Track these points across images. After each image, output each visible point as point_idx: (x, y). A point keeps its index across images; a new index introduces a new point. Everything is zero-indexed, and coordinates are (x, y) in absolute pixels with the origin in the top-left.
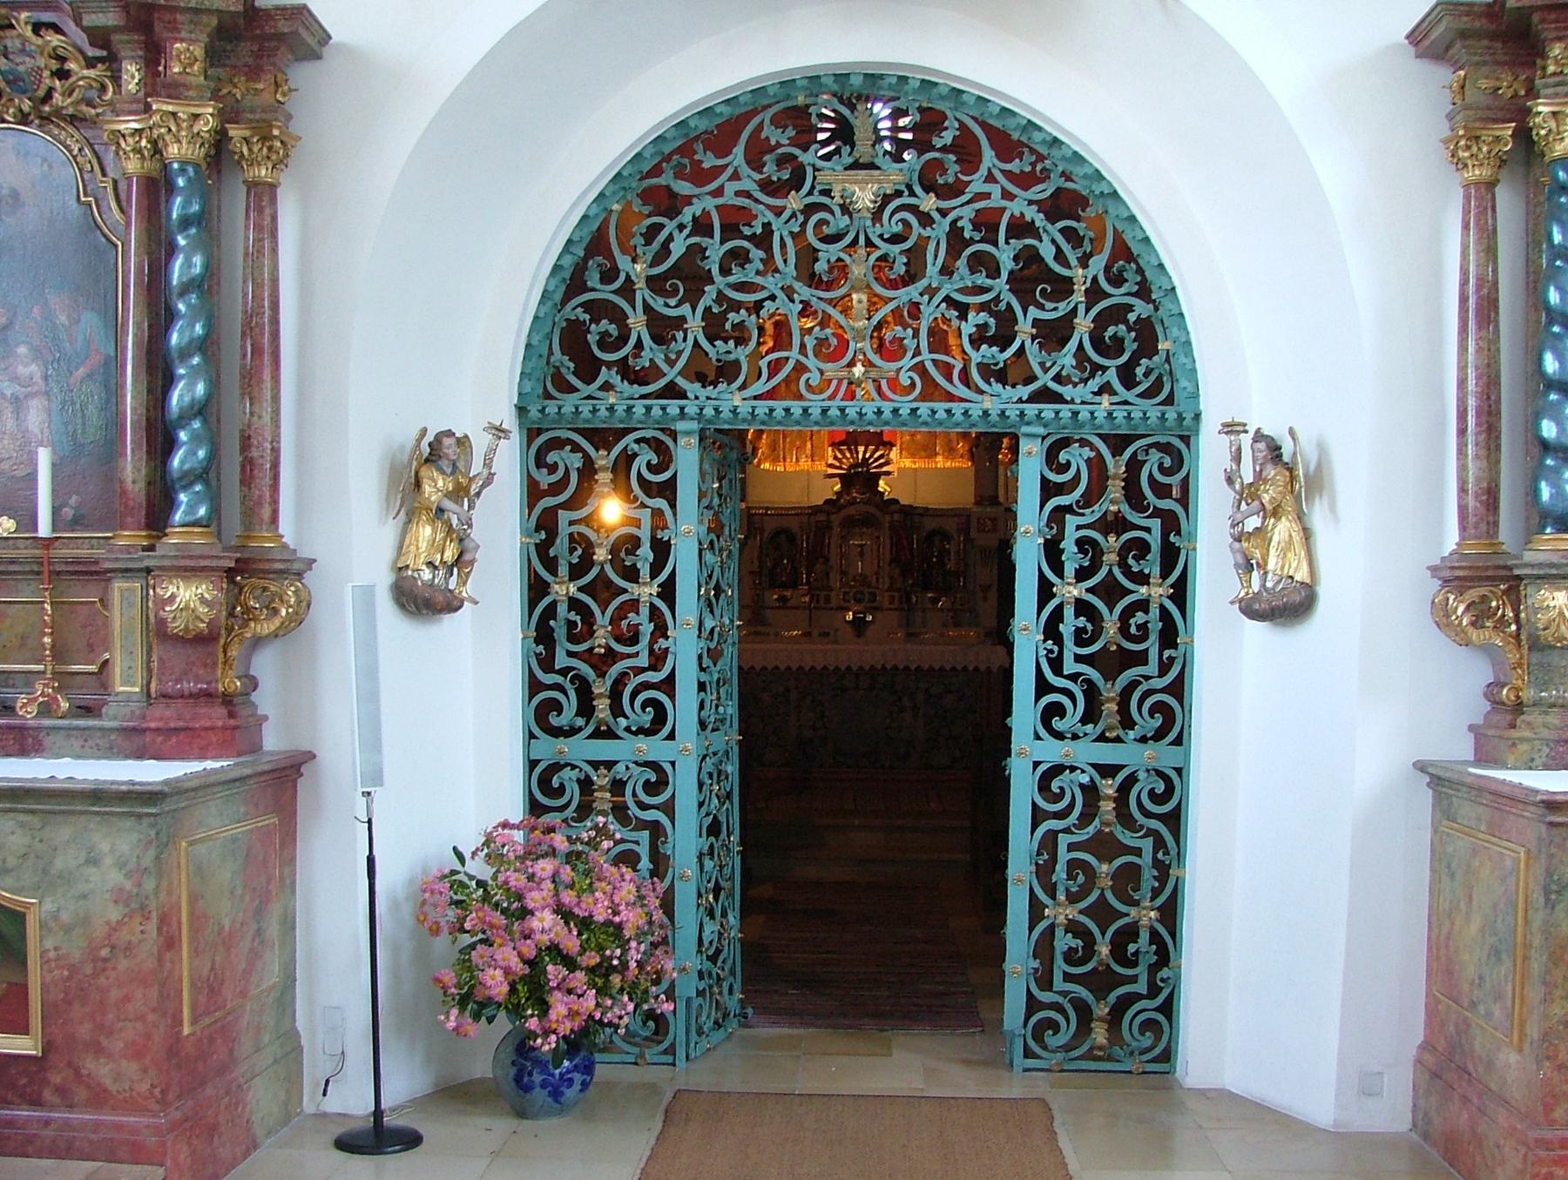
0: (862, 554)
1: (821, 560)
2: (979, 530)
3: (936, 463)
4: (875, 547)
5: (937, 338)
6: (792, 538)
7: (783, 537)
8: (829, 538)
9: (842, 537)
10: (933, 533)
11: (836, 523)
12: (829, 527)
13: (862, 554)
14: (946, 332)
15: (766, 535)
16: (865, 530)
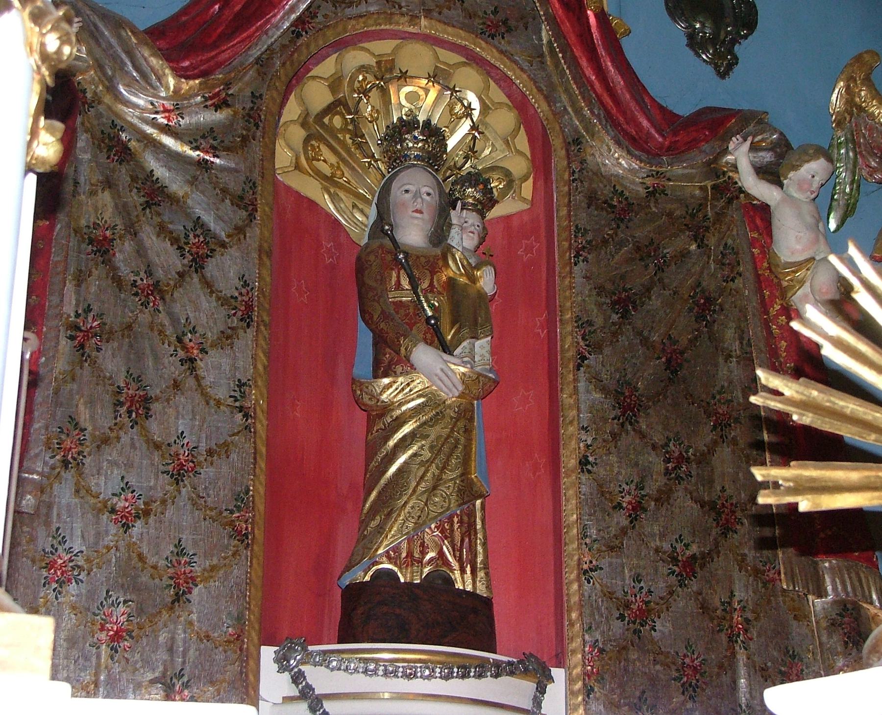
14: (764, 211)
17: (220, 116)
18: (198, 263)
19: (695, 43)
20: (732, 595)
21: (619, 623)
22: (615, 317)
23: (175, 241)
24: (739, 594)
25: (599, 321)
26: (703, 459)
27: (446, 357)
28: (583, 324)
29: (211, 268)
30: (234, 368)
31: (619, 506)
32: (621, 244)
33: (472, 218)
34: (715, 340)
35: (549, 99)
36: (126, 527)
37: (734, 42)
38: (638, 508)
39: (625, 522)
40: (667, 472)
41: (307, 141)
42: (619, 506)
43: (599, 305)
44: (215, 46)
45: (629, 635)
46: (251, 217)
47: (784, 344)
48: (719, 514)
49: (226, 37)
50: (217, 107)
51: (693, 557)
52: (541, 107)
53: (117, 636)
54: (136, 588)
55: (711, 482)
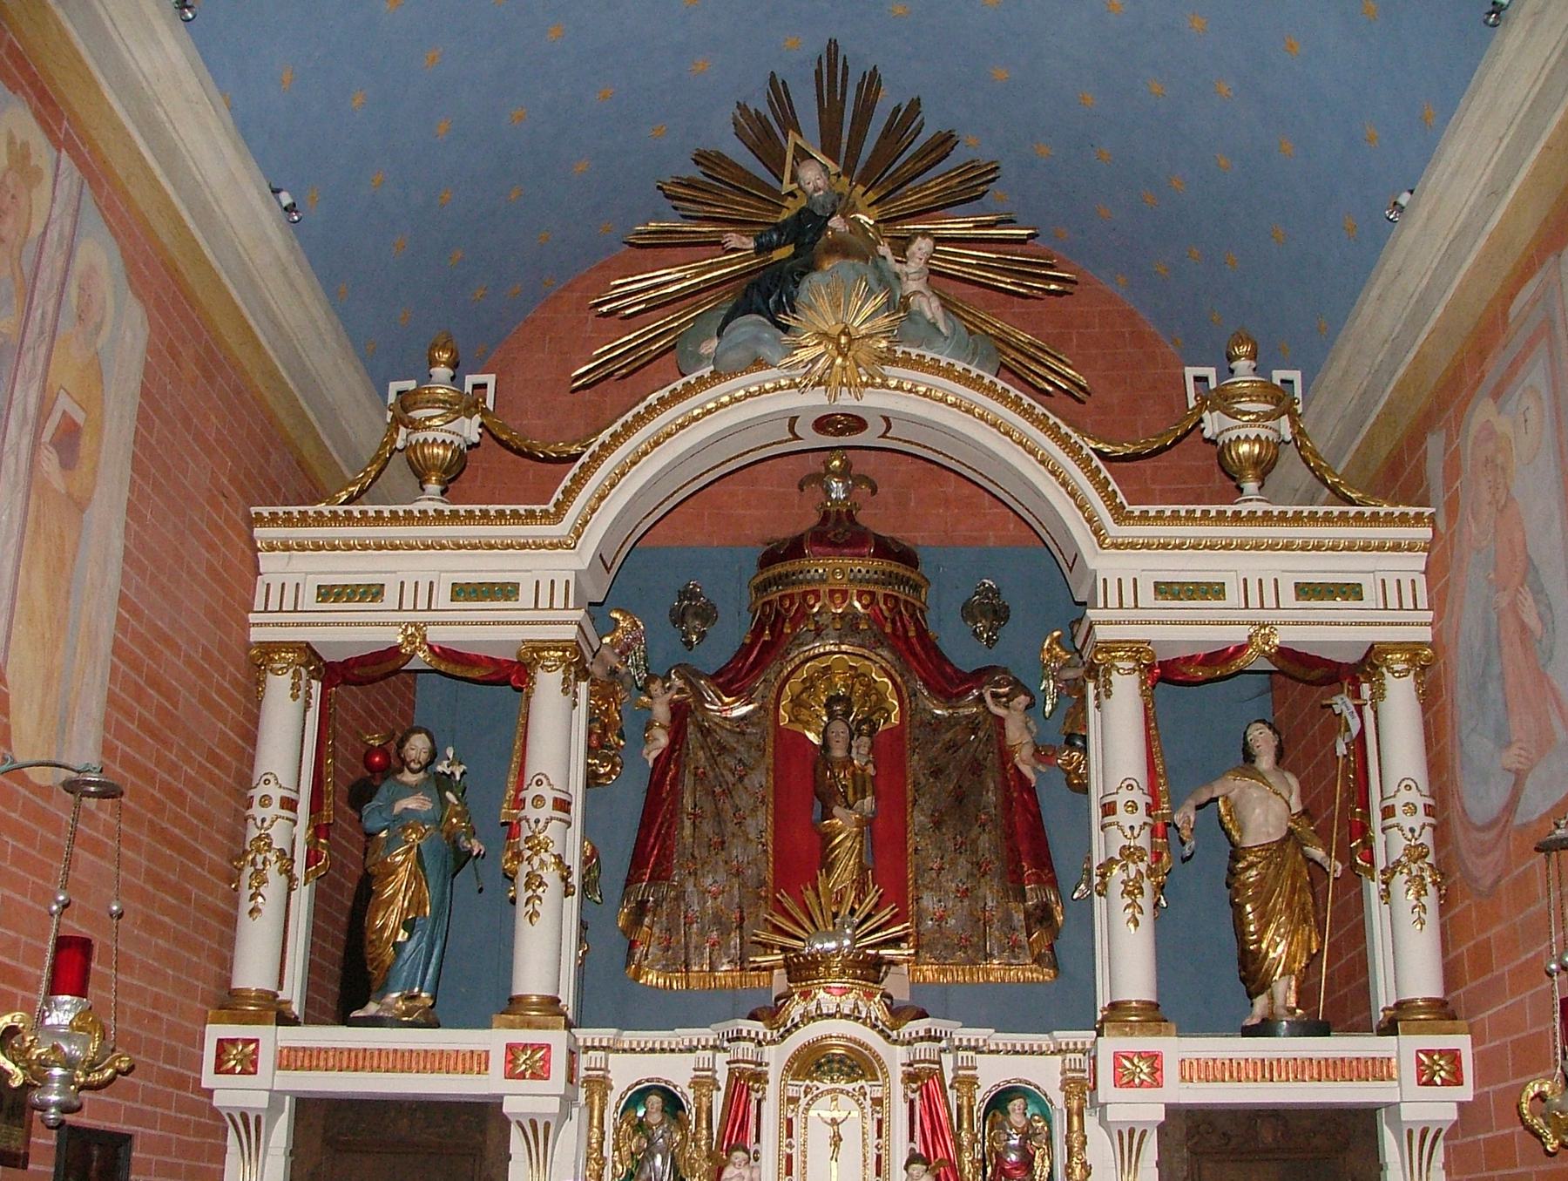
0: (837, 1140)
1: (739, 1155)
2: (1117, 1083)
3: (988, 972)
4: (872, 1127)
5: (981, 734)
6: (672, 1103)
7: (655, 1100)
8: (759, 1102)
9: (794, 1100)
10: (1000, 1100)
11: (774, 1073)
12: (760, 1078)
13: (837, 1140)
14: (1000, 721)
15: (613, 1098)
16: (842, 1085)
17: (751, 707)
18: (741, 779)
19: (978, 636)
20: (986, 904)
21: (930, 922)
22: (931, 780)
23: (731, 770)
24: (990, 904)
25: (923, 780)
26: (974, 842)
27: (848, 811)
28: (916, 784)
29: (746, 781)
30: (757, 824)
31: (932, 869)
32: (934, 743)
33: (865, 739)
34: (981, 783)
35: (901, 675)
36: (716, 898)
37: (997, 629)
38: (941, 868)
39: (934, 875)
40: (956, 850)
41: (793, 709)
42: (932, 869)
43: (924, 774)
44: (743, 679)
45: (936, 927)
46: (764, 755)
47: (1012, 783)
48: (981, 867)
49: (747, 675)
50: (747, 705)
51: (967, 889)
52: (899, 680)
53: (713, 945)
54: (720, 924)
55: (977, 851)
